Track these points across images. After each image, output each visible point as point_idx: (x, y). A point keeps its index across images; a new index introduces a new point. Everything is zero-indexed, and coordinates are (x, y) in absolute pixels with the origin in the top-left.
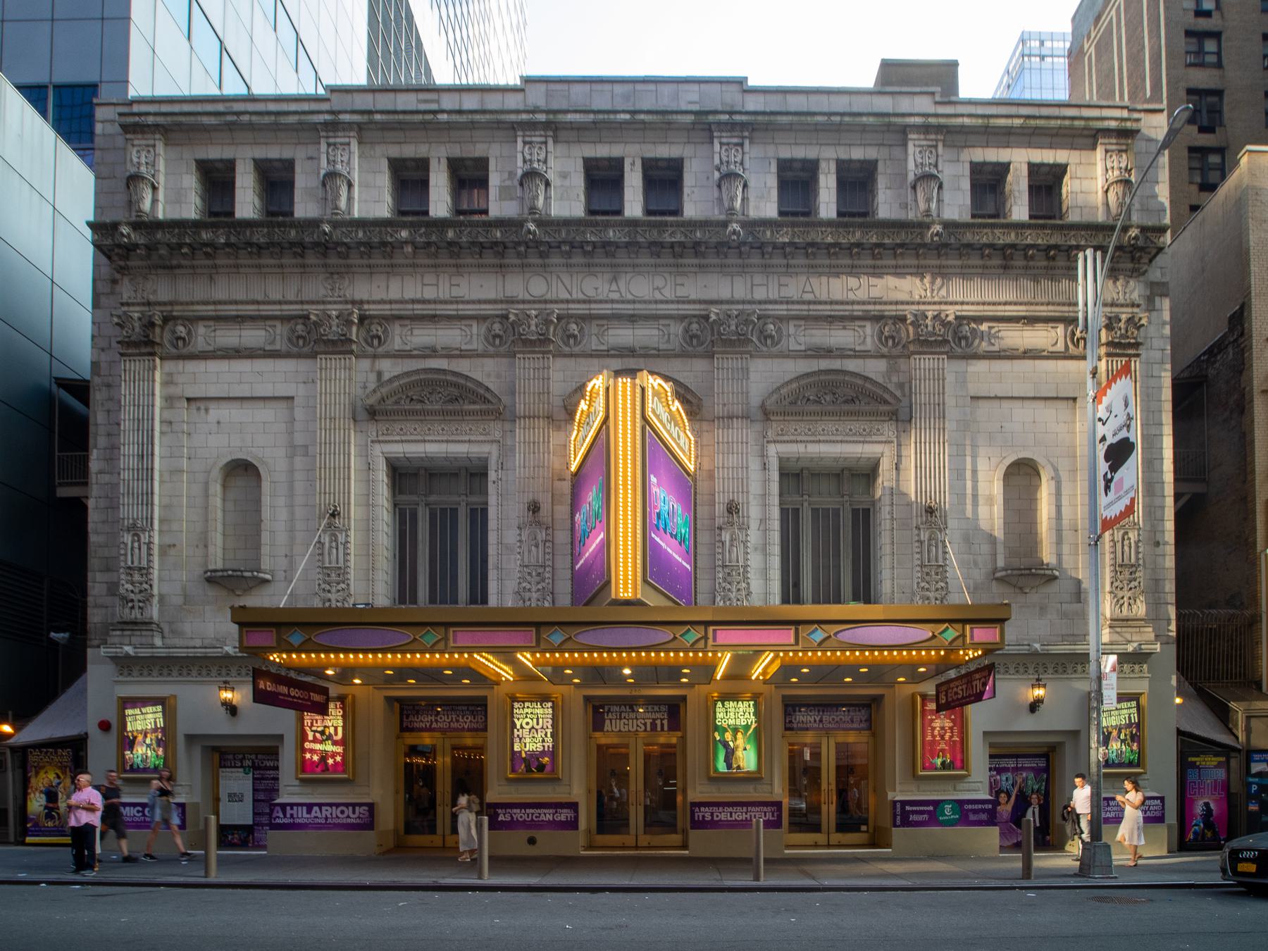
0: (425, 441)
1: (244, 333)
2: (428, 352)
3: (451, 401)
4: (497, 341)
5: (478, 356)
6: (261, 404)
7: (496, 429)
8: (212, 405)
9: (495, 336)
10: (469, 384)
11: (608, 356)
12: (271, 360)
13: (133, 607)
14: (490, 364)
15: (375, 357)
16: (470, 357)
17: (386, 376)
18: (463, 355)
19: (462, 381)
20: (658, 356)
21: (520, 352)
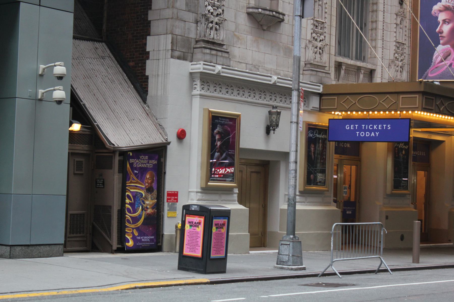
13: (211, 28)
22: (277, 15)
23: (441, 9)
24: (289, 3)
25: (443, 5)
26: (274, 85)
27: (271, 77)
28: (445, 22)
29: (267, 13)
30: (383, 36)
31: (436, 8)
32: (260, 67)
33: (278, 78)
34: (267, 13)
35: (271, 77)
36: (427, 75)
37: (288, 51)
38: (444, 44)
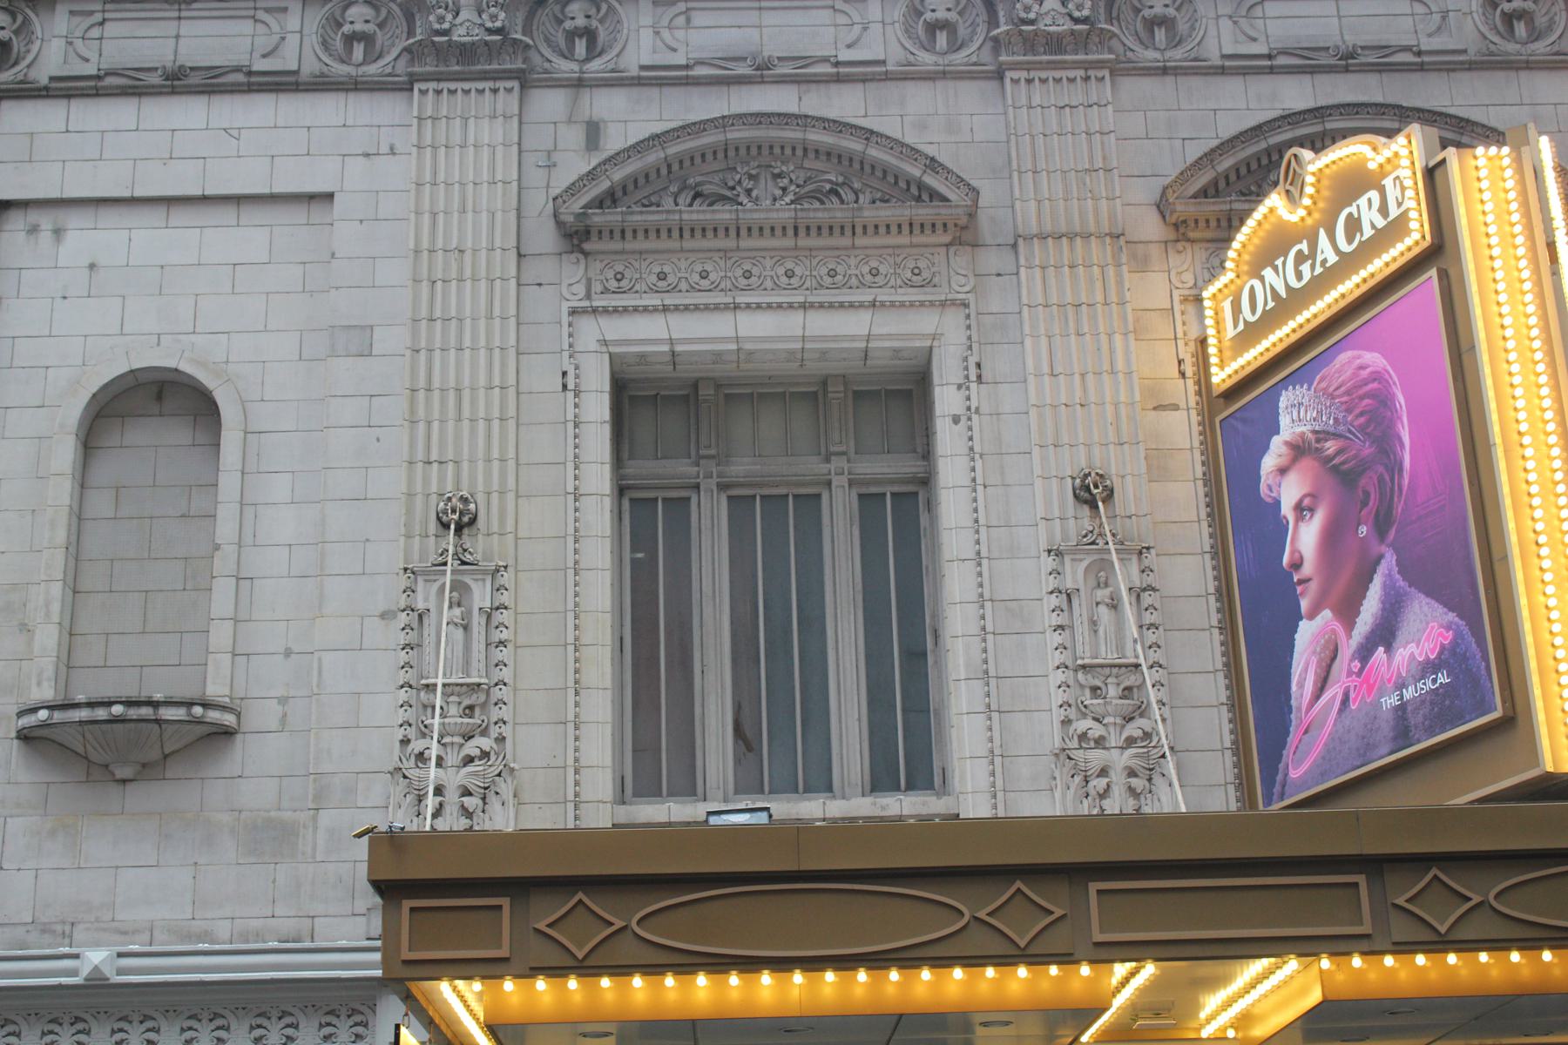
0: (736, 307)
1: (186, 28)
2: (742, 70)
3: (818, 196)
4: (942, 39)
5: (888, 77)
6: (227, 214)
7: (956, 274)
8: (75, 220)
9: (933, 28)
10: (874, 152)
11: (1272, 70)
12: (273, 96)
14: (919, 98)
15: (579, 84)
16: (864, 81)
17: (614, 141)
18: (842, 75)
19: (854, 145)
20: (1421, 68)
21: (1015, 66)
22: (146, 712)
23: (1283, 461)
24: (288, 653)
25: (1287, 443)
26: (97, 985)
27: (77, 956)
28: (1302, 510)
29: (84, 714)
30: (986, 662)
31: (1269, 463)
32: (81, 927)
33: (120, 955)
34: (84, 714)
35: (77, 956)
36: (1286, 775)
37: (272, 837)
38: (1312, 615)
